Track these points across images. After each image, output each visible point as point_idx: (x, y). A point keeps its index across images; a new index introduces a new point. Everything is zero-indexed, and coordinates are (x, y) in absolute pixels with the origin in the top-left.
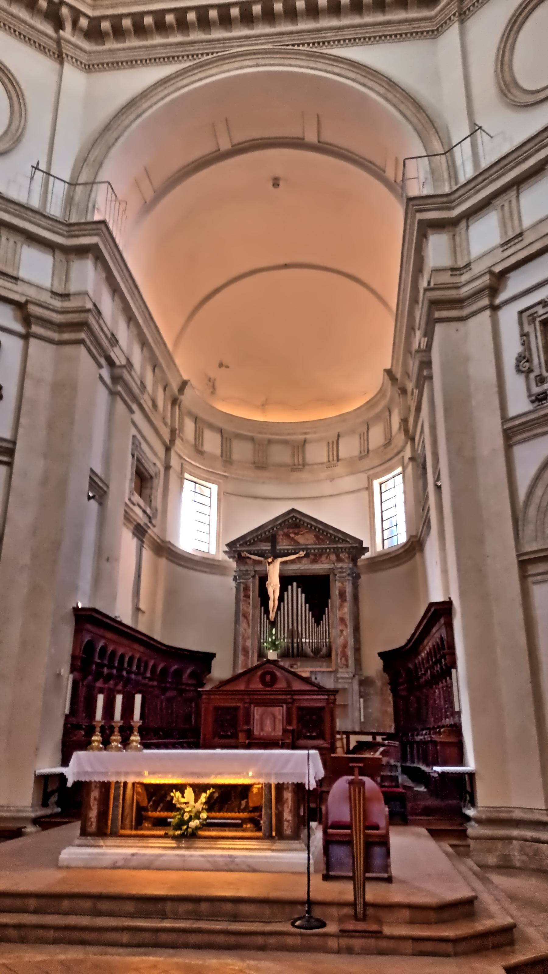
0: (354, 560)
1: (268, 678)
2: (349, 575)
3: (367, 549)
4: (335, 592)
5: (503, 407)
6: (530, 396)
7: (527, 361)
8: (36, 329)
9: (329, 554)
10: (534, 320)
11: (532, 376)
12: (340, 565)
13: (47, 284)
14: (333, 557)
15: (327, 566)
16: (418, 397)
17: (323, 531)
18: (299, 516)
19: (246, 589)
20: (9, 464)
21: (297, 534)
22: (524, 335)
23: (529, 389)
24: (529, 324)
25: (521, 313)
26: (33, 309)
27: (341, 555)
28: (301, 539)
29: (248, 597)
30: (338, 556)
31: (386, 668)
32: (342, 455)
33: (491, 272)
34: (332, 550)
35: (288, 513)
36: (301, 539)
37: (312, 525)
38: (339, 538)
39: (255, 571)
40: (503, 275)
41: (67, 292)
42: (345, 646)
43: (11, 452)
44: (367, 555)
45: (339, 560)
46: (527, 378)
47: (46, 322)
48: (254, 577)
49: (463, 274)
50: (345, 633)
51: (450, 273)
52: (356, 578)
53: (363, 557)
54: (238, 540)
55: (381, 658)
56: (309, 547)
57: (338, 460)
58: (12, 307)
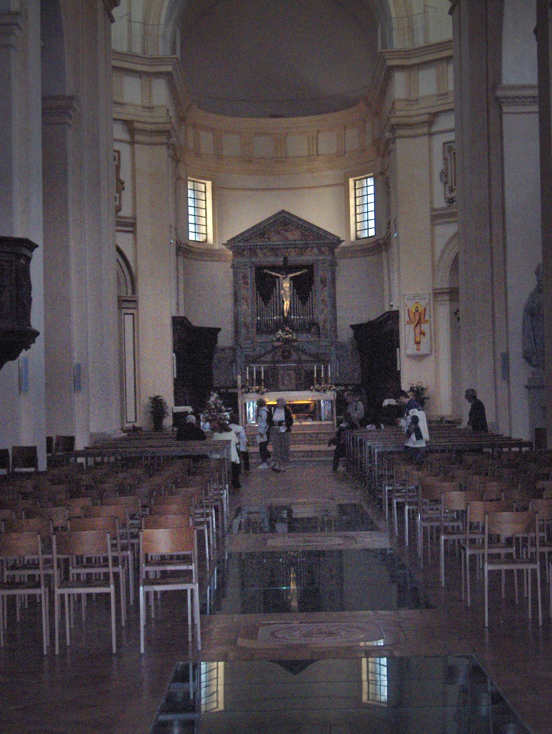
0: (332, 252)
1: (286, 353)
2: (329, 265)
3: (343, 241)
4: (317, 279)
5: (431, 202)
6: (445, 198)
7: (446, 176)
8: (138, 138)
9: (312, 248)
10: (451, 150)
11: (447, 186)
12: (321, 257)
13: (139, 102)
14: (316, 251)
15: (311, 258)
16: (391, 30)
17: (308, 229)
18: (288, 217)
19: (245, 277)
20: (134, 232)
21: (286, 231)
22: (445, 159)
23: (445, 194)
24: (448, 153)
25: (444, 144)
26: (136, 125)
27: (323, 248)
28: (290, 236)
29: (246, 283)
30: (319, 250)
31: (356, 337)
32: (321, 151)
33: (429, 114)
34: (315, 245)
35: (279, 213)
36: (290, 236)
37: (298, 224)
38: (321, 235)
39: (252, 262)
40: (436, 114)
41: (152, 106)
42: (325, 321)
43: (134, 225)
44: (343, 244)
45: (321, 253)
46: (445, 186)
47: (143, 132)
48: (251, 267)
49: (414, 104)
50: (325, 312)
51: (406, 103)
52: (333, 264)
53: (339, 246)
54: (237, 237)
55: (353, 329)
56: (297, 242)
57: (318, 155)
58: (122, 122)
